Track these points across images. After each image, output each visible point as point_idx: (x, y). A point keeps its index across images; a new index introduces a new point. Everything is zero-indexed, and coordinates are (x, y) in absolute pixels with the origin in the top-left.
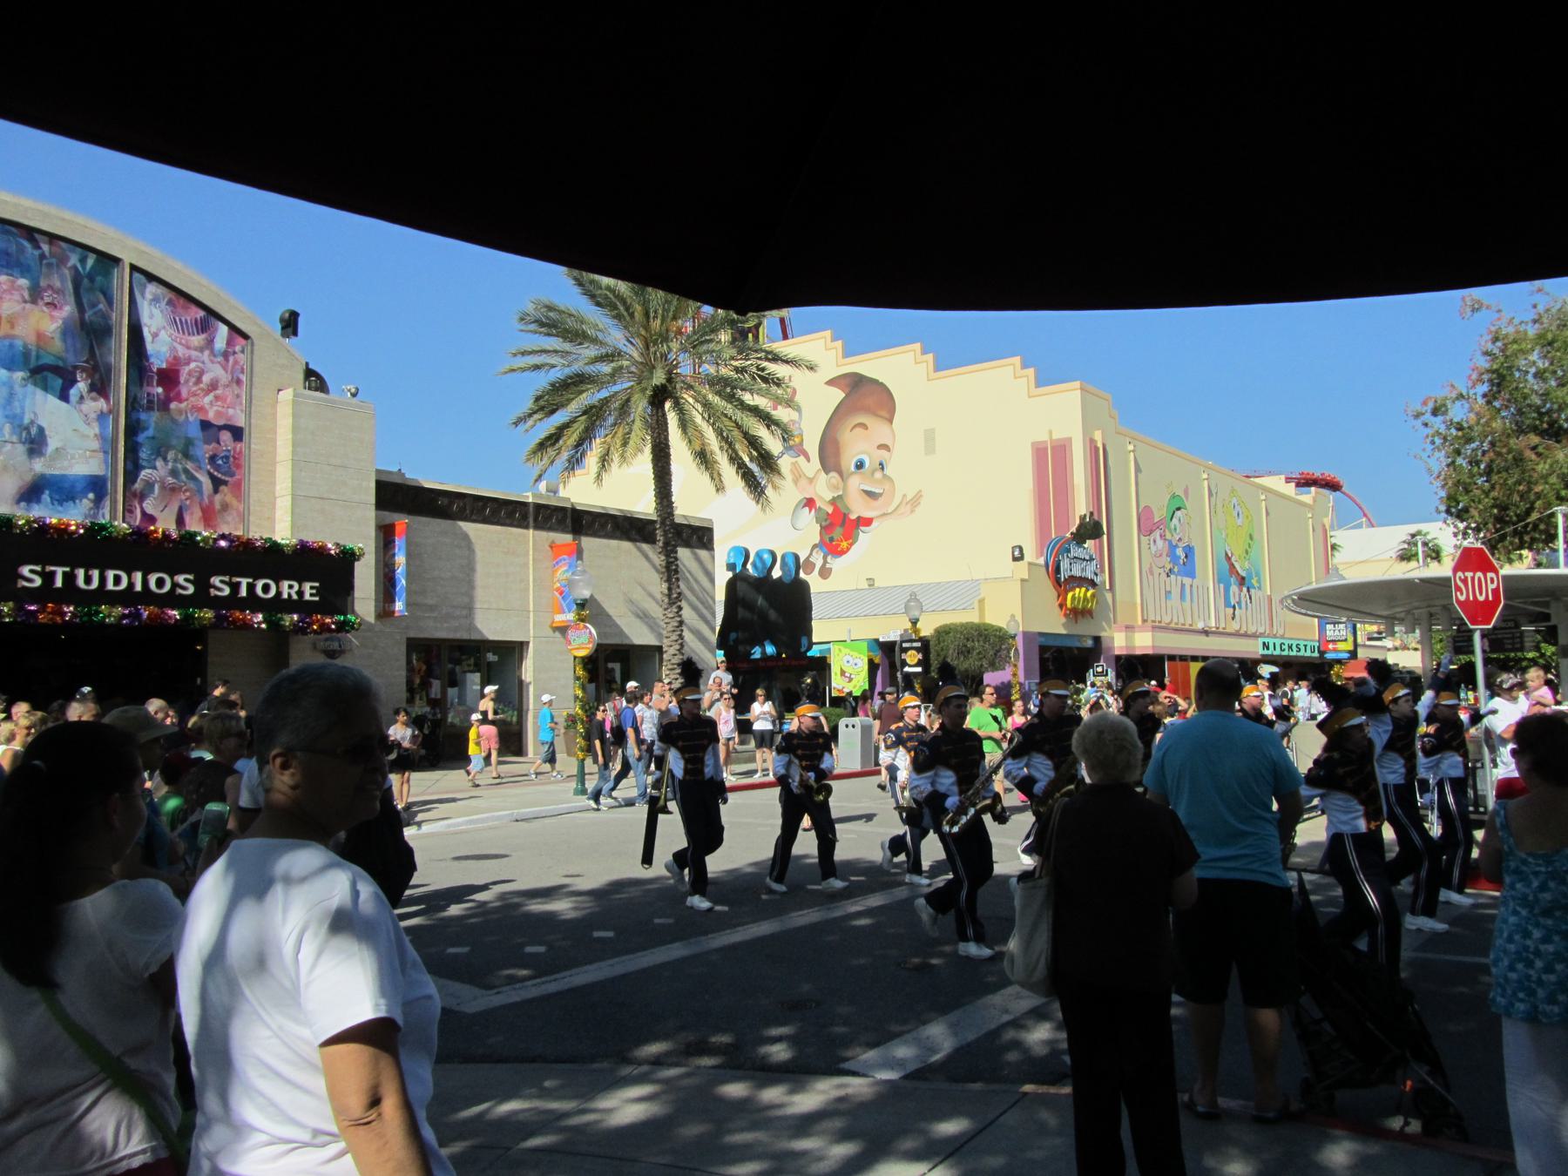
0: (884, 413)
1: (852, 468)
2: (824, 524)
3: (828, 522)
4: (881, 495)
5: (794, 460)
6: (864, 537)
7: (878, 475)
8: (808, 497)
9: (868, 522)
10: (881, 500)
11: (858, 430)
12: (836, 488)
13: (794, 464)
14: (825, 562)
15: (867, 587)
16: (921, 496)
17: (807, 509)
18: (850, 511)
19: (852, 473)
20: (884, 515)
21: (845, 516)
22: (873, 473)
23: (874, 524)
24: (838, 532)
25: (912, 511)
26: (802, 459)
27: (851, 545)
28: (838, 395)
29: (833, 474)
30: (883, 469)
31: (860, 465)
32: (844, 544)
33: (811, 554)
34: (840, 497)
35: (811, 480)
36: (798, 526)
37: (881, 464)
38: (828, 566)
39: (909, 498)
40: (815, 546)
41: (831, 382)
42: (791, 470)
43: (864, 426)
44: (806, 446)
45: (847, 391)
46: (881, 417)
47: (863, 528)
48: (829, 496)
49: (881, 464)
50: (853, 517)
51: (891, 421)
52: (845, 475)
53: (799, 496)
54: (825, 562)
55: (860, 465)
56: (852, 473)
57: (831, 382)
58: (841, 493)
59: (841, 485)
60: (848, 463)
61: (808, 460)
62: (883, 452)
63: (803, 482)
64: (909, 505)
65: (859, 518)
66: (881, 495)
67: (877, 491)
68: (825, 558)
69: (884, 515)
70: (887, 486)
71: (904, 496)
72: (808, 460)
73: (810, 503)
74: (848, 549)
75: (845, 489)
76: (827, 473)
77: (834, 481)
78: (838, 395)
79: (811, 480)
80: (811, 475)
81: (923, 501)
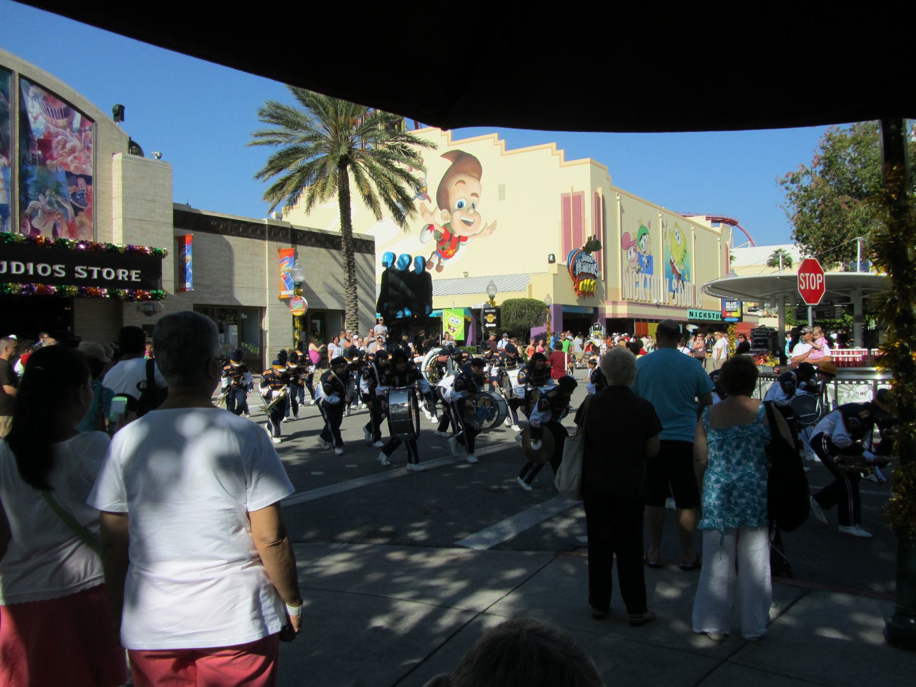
1: (456, 207)
2: (439, 239)
3: (442, 238)
4: (472, 223)
5: (422, 201)
6: (463, 248)
7: (471, 211)
8: (430, 223)
10: (473, 226)
11: (460, 184)
12: (446, 218)
13: (422, 204)
14: (440, 262)
15: (464, 277)
16: (496, 224)
17: (429, 230)
19: (456, 210)
20: (474, 235)
21: (452, 235)
22: (468, 210)
23: (469, 240)
24: (447, 245)
25: (491, 233)
26: (426, 201)
27: (455, 252)
28: (448, 163)
29: (445, 210)
30: (474, 207)
32: (451, 252)
33: (431, 257)
34: (449, 224)
35: (432, 214)
36: (424, 240)
37: (473, 205)
38: (441, 264)
39: (489, 225)
40: (433, 253)
41: (445, 155)
43: (463, 182)
44: (429, 193)
46: (473, 177)
48: (442, 224)
49: (473, 205)
50: (456, 236)
51: (479, 179)
52: (452, 211)
54: (440, 262)
56: (456, 210)
57: (445, 155)
58: (449, 221)
59: (449, 216)
60: (454, 204)
61: (430, 202)
62: (475, 198)
63: (427, 215)
66: (472, 223)
67: (471, 221)
68: (439, 260)
69: (474, 235)
71: (486, 224)
72: (430, 202)
73: (431, 227)
74: (453, 255)
78: (448, 163)
79: (432, 214)
80: (432, 211)
81: (497, 227)
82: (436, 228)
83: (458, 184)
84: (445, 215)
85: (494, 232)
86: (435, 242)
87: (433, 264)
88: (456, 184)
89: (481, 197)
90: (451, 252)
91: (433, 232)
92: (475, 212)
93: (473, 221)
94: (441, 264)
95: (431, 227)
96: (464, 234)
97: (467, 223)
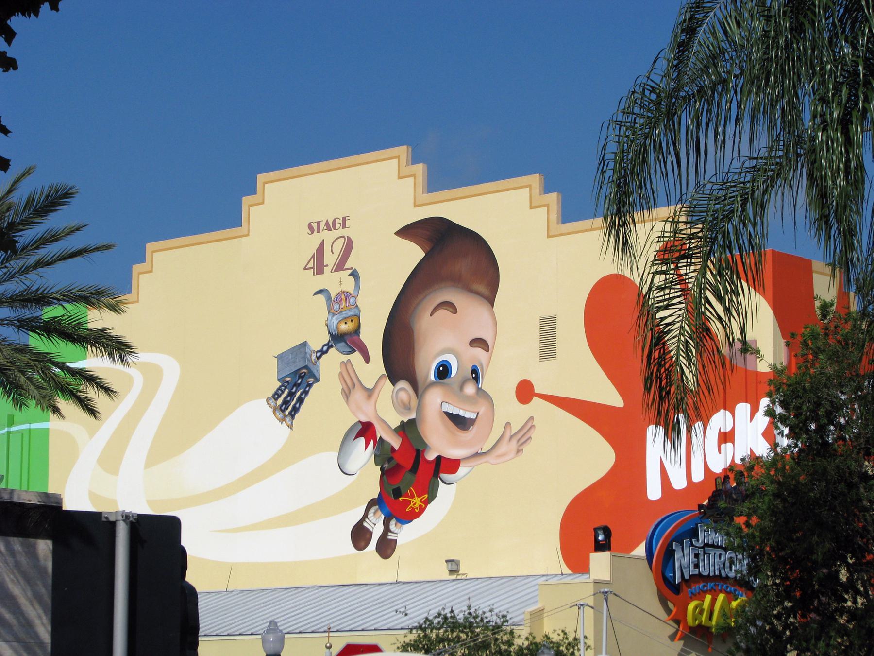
0: (482, 288)
1: (432, 377)
2: (386, 466)
3: (393, 463)
4: (472, 422)
5: (345, 358)
6: (446, 493)
7: (470, 389)
8: (364, 419)
9: (453, 465)
10: (473, 430)
11: (443, 313)
12: (407, 408)
13: (346, 364)
14: (387, 530)
15: (446, 576)
16: (533, 426)
17: (362, 441)
18: (425, 445)
19: (432, 384)
20: (477, 455)
21: (419, 454)
22: (461, 388)
23: (462, 470)
24: (406, 480)
25: (518, 451)
26: (356, 358)
27: (427, 502)
28: (413, 254)
29: (403, 384)
30: (476, 379)
31: (443, 371)
32: (417, 501)
33: (366, 515)
34: (412, 422)
35: (370, 393)
36: (350, 467)
37: (475, 371)
38: (391, 536)
39: (515, 429)
40: (371, 504)
41: (408, 232)
42: (341, 374)
43: (449, 306)
44: (364, 336)
45: (428, 249)
46: (477, 293)
47: (443, 476)
48: (395, 422)
49: (475, 371)
50: (431, 456)
53: (349, 419)
54: (387, 530)
55: (443, 371)
56: (432, 384)
57: (408, 232)
58: (413, 416)
59: (414, 402)
60: (427, 369)
61: (367, 360)
62: (479, 352)
63: (358, 395)
64: (514, 442)
65: (439, 458)
66: (472, 422)
67: (468, 415)
68: (386, 524)
69: (477, 455)
70: (483, 409)
71: (508, 424)
72: (367, 360)
73: (366, 430)
74: (422, 510)
75: (420, 409)
76: (394, 382)
77: (403, 396)
78: (413, 254)
79: (370, 393)
80: (369, 385)
81: (535, 434)
82: (380, 433)
83: (436, 314)
84: (403, 396)
85: (526, 448)
86: (377, 472)
87: (371, 533)
88: (431, 315)
89: (500, 349)
90: (417, 501)
91: (372, 443)
92: (479, 390)
93: (473, 416)
94: (391, 536)
95: (366, 430)
96: (452, 453)
97: (459, 422)
